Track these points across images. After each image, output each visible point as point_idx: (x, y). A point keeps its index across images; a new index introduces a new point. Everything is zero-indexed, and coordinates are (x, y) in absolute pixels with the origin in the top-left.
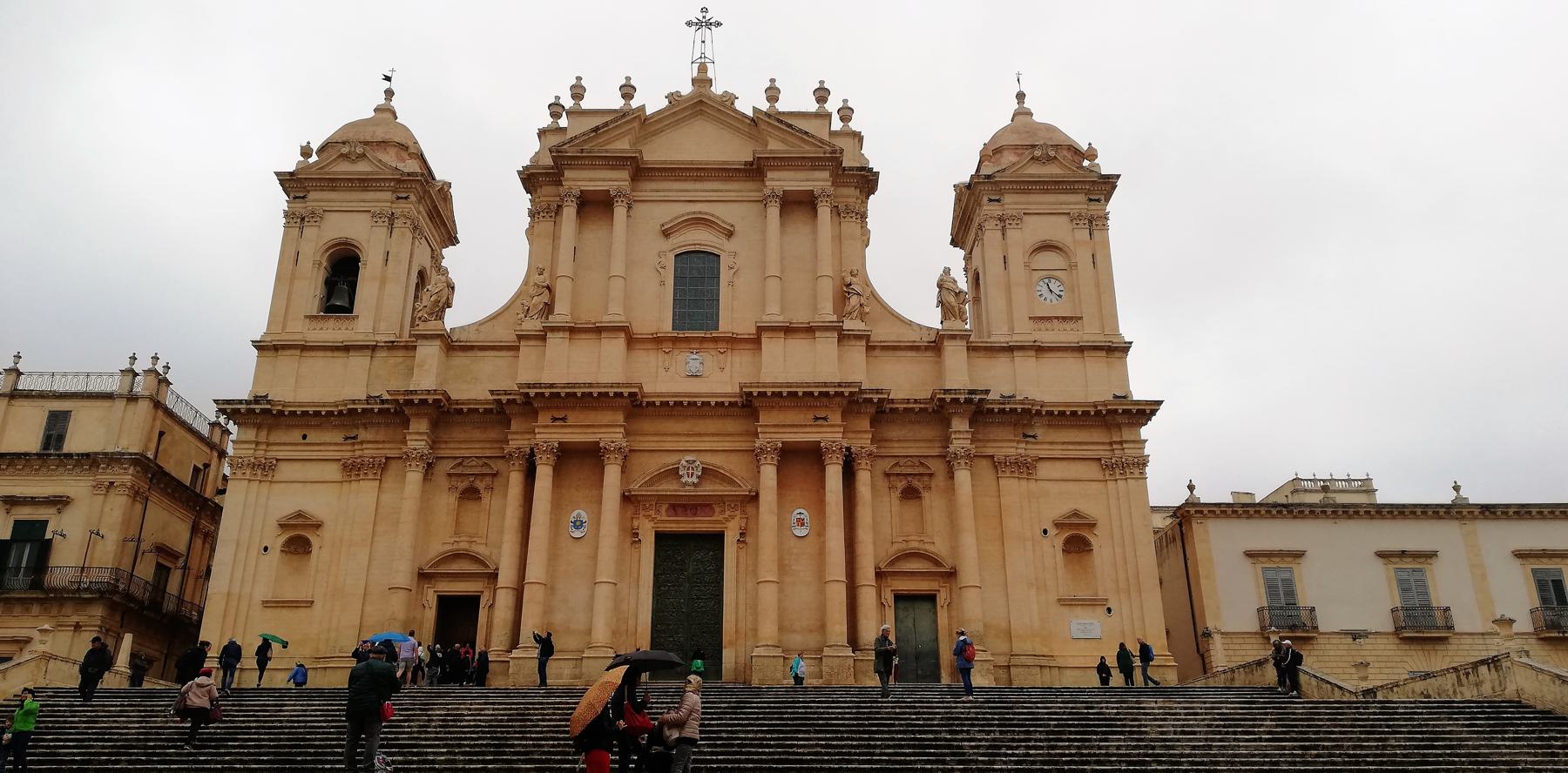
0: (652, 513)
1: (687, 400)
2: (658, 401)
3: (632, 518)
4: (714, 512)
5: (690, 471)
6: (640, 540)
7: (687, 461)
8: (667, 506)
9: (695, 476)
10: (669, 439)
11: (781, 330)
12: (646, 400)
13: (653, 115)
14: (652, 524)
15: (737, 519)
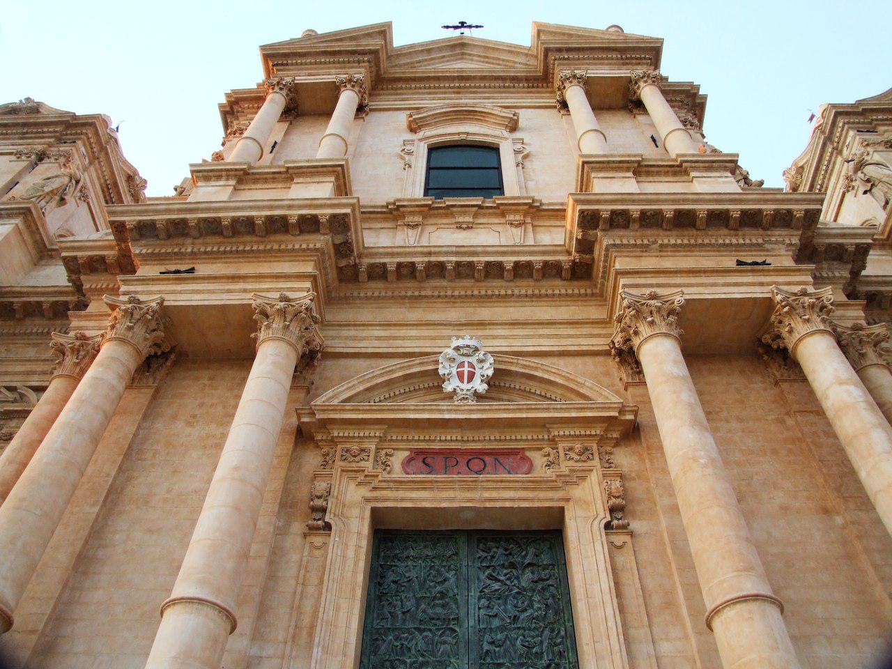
0: (368, 465)
1: (454, 259)
2: (391, 262)
3: (315, 476)
4: (532, 465)
5: (466, 369)
6: (328, 527)
7: (457, 349)
8: (407, 453)
9: (477, 380)
10: (414, 332)
11: (628, 170)
12: (367, 261)
13: (402, 48)
14: (365, 492)
15: (594, 477)
